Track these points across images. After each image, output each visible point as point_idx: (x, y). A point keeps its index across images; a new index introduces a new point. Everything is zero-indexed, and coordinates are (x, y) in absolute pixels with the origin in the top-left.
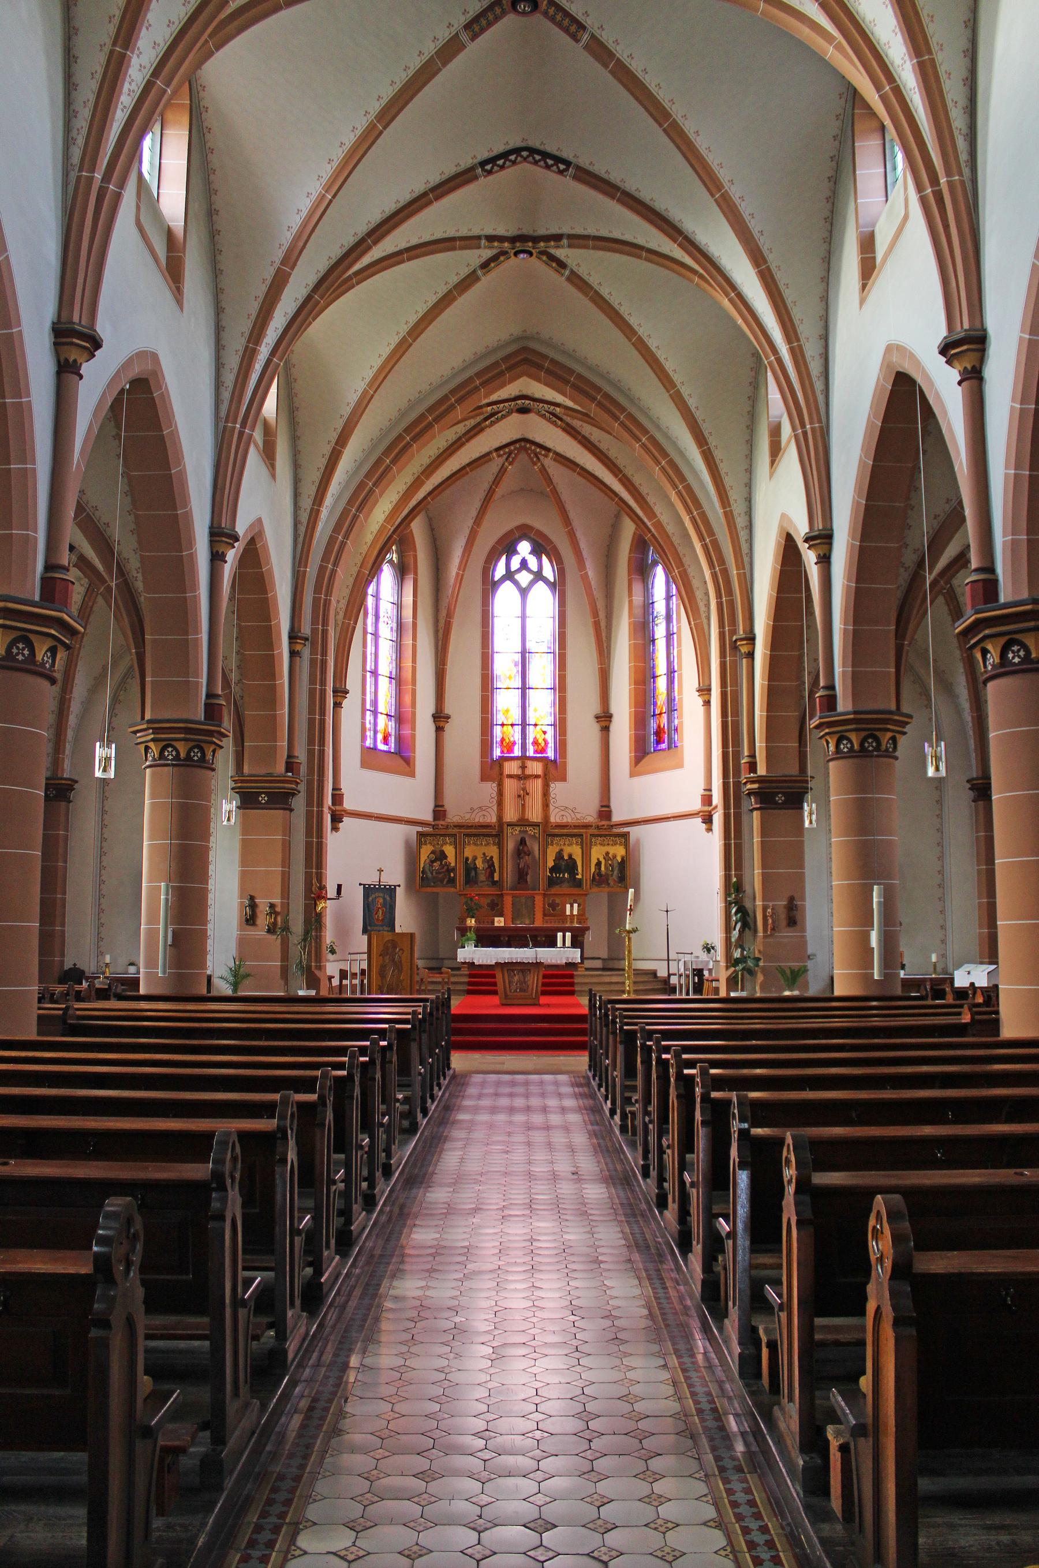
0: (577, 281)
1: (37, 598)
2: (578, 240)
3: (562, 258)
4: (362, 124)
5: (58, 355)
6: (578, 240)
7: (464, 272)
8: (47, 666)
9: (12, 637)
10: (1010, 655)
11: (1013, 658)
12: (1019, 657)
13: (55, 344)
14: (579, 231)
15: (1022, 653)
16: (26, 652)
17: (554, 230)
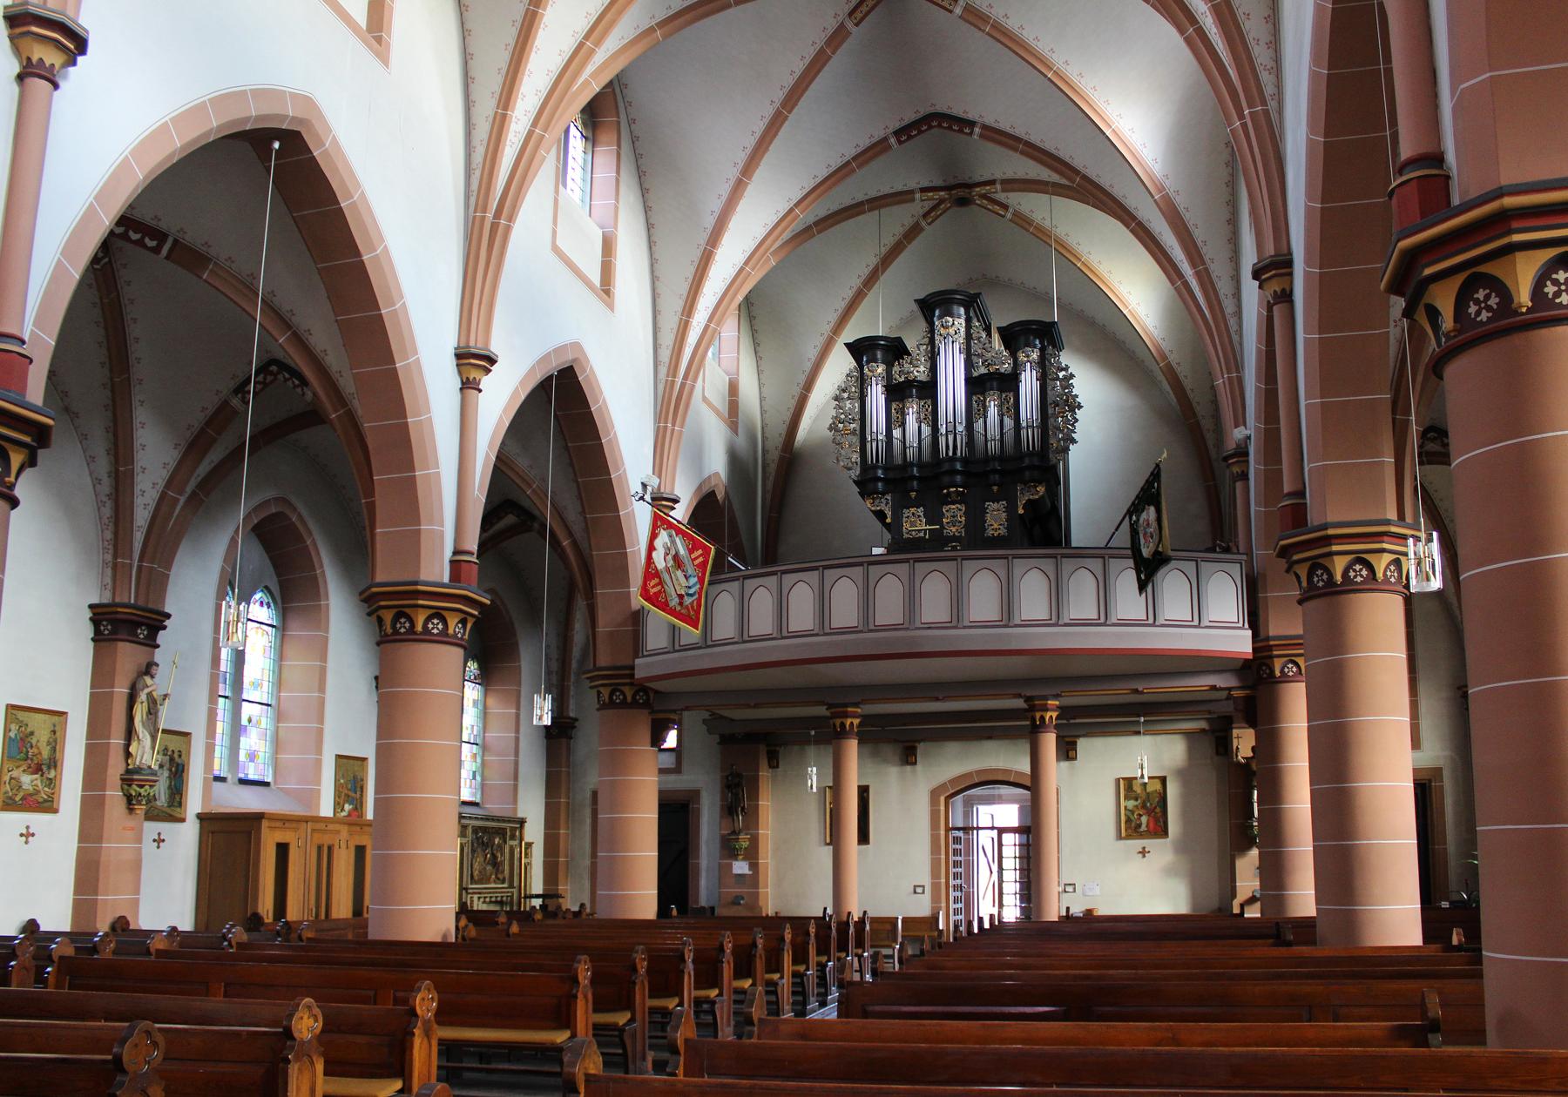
0: (1022, 221)
1: (446, 579)
2: (1012, 184)
3: (1004, 201)
4: (769, 111)
5: (460, 373)
6: (1012, 184)
7: (909, 222)
8: (459, 635)
9: (427, 615)
10: (1316, 579)
11: (1318, 582)
12: (1323, 580)
13: (457, 365)
14: (1010, 174)
15: (1325, 577)
16: (440, 626)
17: (987, 177)
